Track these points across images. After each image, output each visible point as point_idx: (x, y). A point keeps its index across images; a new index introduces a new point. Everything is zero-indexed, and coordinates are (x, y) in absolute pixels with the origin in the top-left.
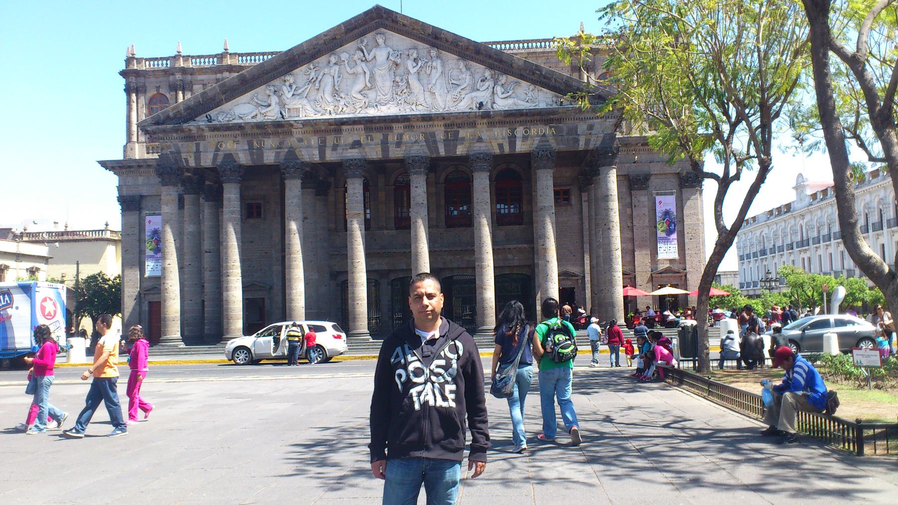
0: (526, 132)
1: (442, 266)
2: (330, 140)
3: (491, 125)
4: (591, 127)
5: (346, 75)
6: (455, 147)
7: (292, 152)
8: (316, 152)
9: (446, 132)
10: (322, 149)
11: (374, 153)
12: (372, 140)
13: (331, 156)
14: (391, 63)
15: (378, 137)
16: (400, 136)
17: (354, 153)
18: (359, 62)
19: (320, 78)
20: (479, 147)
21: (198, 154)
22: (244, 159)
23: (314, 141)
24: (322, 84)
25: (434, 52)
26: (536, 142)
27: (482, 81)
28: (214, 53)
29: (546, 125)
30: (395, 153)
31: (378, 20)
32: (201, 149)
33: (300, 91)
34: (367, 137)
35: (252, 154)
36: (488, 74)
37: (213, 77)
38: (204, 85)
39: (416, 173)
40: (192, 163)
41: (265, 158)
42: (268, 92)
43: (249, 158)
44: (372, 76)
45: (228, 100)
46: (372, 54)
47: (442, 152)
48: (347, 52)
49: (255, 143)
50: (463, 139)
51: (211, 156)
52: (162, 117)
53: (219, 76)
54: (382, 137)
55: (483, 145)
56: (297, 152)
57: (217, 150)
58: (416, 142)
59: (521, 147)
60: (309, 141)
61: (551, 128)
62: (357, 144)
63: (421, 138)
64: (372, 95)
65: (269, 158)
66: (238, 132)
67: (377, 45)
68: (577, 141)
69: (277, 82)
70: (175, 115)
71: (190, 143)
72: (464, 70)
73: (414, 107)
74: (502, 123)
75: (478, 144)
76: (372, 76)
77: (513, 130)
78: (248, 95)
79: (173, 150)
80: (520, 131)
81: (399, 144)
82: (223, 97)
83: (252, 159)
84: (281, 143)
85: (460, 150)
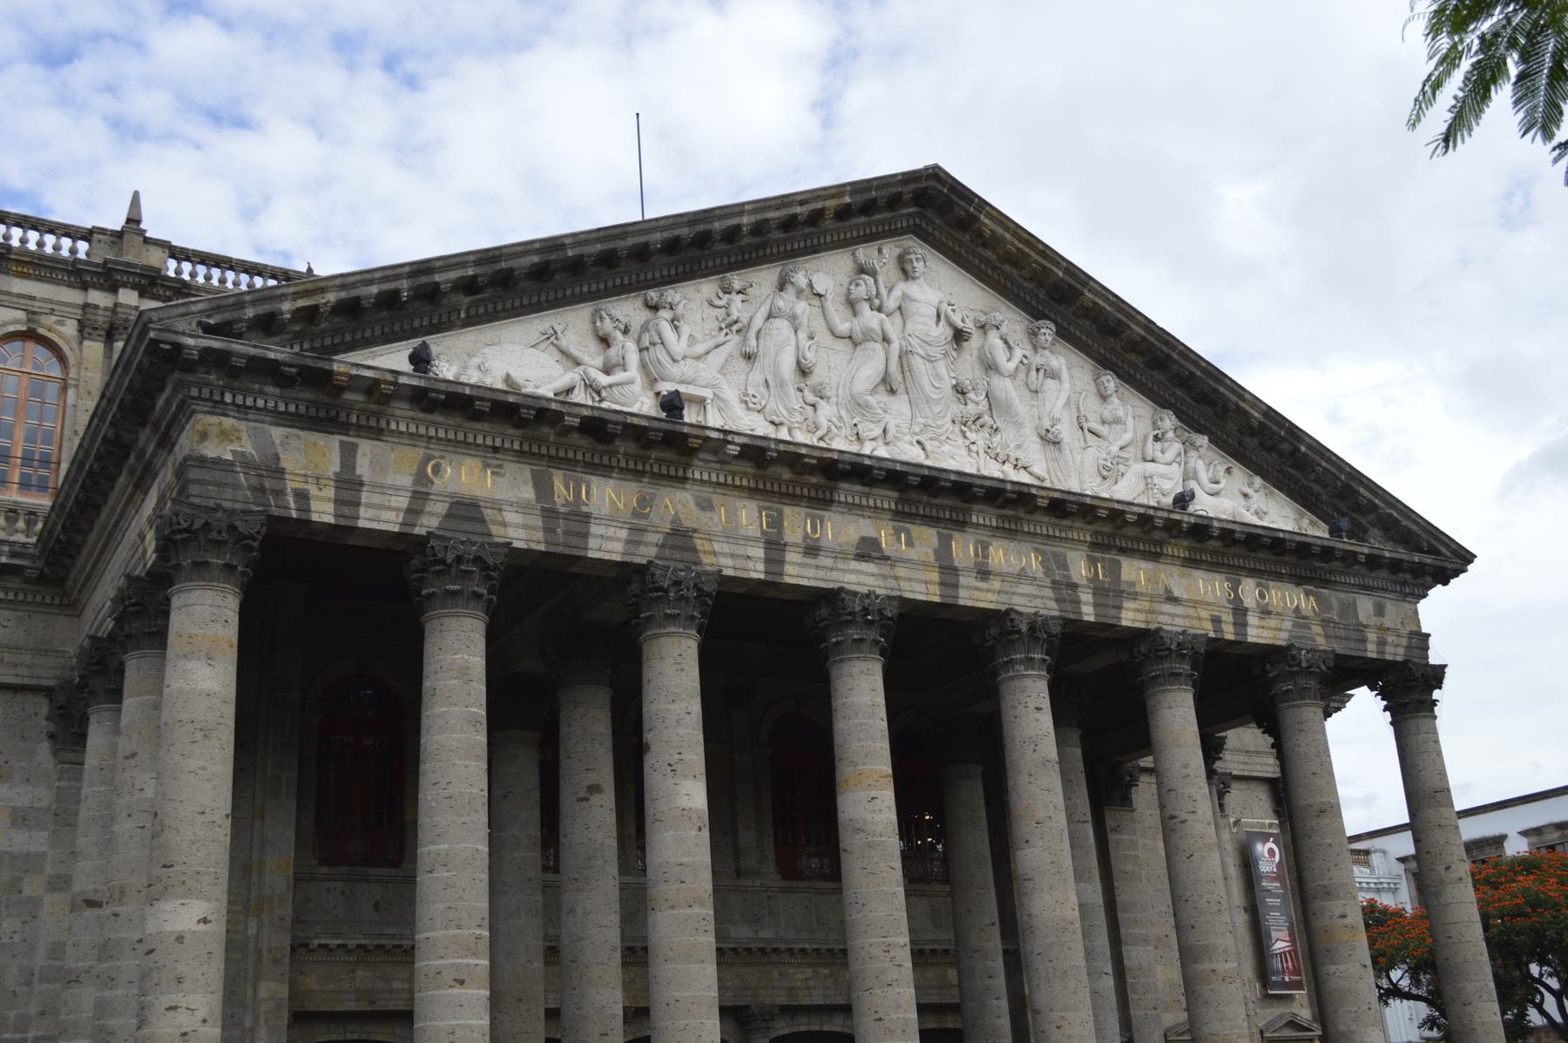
0: (1262, 596)
1: (782, 1000)
2: (796, 523)
3: (1192, 563)
4: (1380, 611)
5: (828, 337)
6: (1119, 608)
7: (680, 537)
8: (759, 552)
9: (1092, 561)
10: (775, 547)
11: (923, 588)
12: (910, 544)
13: (799, 572)
14: (949, 333)
15: (926, 538)
16: (985, 547)
17: (860, 578)
18: (865, 307)
19: (758, 322)
20: (1172, 620)
21: (349, 486)
22: (519, 529)
23: (748, 515)
24: (768, 344)
25: (1047, 331)
26: (1288, 625)
27: (1156, 438)
28: (88, 223)
29: (1298, 584)
30: (975, 595)
31: (930, 211)
32: (363, 469)
33: (700, 349)
34: (897, 532)
35: (550, 514)
36: (1169, 421)
37: (74, 296)
38: (32, 314)
39: (1029, 662)
40: (323, 511)
41: (592, 543)
42: (607, 326)
43: (540, 535)
44: (904, 355)
45: (473, 321)
46: (897, 293)
47: (1088, 614)
48: (827, 273)
49: (558, 484)
50: (1133, 584)
51: (403, 502)
52: (250, 313)
53: (98, 298)
54: (935, 541)
55: (1179, 610)
56: (699, 543)
57: (421, 477)
58: (1022, 576)
59: (1258, 633)
60: (732, 514)
61: (1307, 594)
62: (868, 551)
63: (1034, 564)
64: (900, 405)
65: (607, 544)
66: (512, 438)
67: (906, 274)
68: (1364, 641)
69: (628, 310)
70: (297, 313)
71: (320, 439)
72: (1114, 399)
73: (1008, 468)
74: (1214, 567)
75: (1168, 608)
76: (904, 355)
77: (1235, 589)
78: (536, 325)
79: (248, 447)
80: (1249, 590)
81: (984, 573)
82: (464, 300)
83: (548, 530)
84: (644, 502)
85: (1131, 617)
